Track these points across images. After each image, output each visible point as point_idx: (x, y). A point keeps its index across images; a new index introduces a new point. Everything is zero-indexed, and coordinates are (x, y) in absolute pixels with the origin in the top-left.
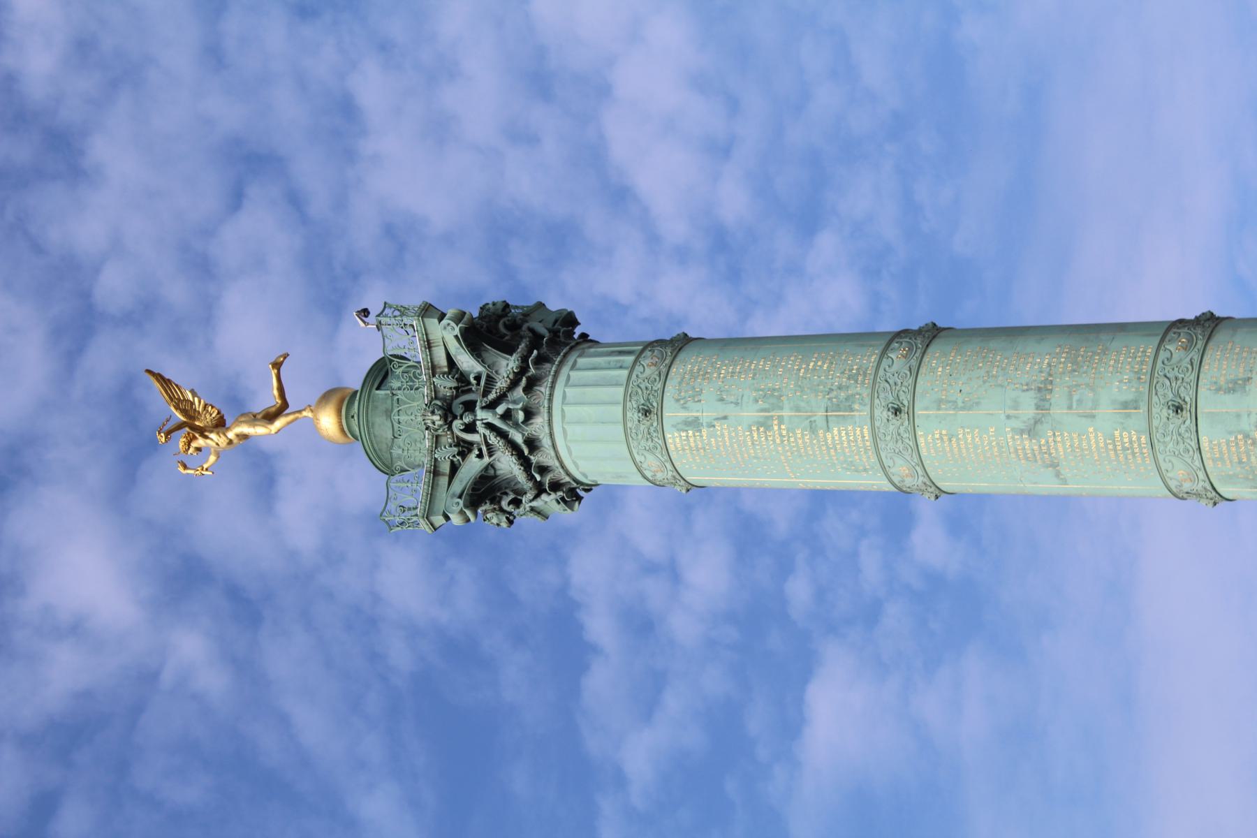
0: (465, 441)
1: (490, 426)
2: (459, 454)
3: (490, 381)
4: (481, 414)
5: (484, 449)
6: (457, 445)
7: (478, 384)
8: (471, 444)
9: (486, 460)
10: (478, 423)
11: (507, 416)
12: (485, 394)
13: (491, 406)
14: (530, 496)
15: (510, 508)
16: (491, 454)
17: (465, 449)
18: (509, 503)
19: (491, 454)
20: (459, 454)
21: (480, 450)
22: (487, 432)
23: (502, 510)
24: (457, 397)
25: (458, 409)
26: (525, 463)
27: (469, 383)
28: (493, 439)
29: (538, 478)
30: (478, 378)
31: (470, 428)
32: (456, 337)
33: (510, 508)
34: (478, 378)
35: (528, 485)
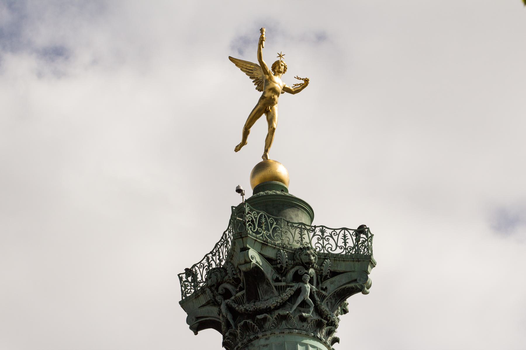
0: (287, 272)
1: (299, 292)
2: (282, 266)
3: (323, 297)
4: (308, 286)
5: (283, 284)
6: (286, 268)
7: (322, 289)
8: (285, 275)
9: (273, 284)
10: (301, 284)
11: (304, 304)
12: (318, 293)
13: (311, 296)
14: (235, 306)
16: (279, 289)
17: (281, 271)
18: (226, 289)
19: (279, 289)
20: (282, 266)
21: (280, 281)
22: (294, 289)
23: (219, 284)
24: (316, 272)
25: (311, 271)
26: (269, 311)
27: (322, 282)
28: (289, 292)
29: (259, 317)
30: (325, 289)
31: (298, 278)
32: (355, 281)
34: (325, 289)
35: (250, 307)
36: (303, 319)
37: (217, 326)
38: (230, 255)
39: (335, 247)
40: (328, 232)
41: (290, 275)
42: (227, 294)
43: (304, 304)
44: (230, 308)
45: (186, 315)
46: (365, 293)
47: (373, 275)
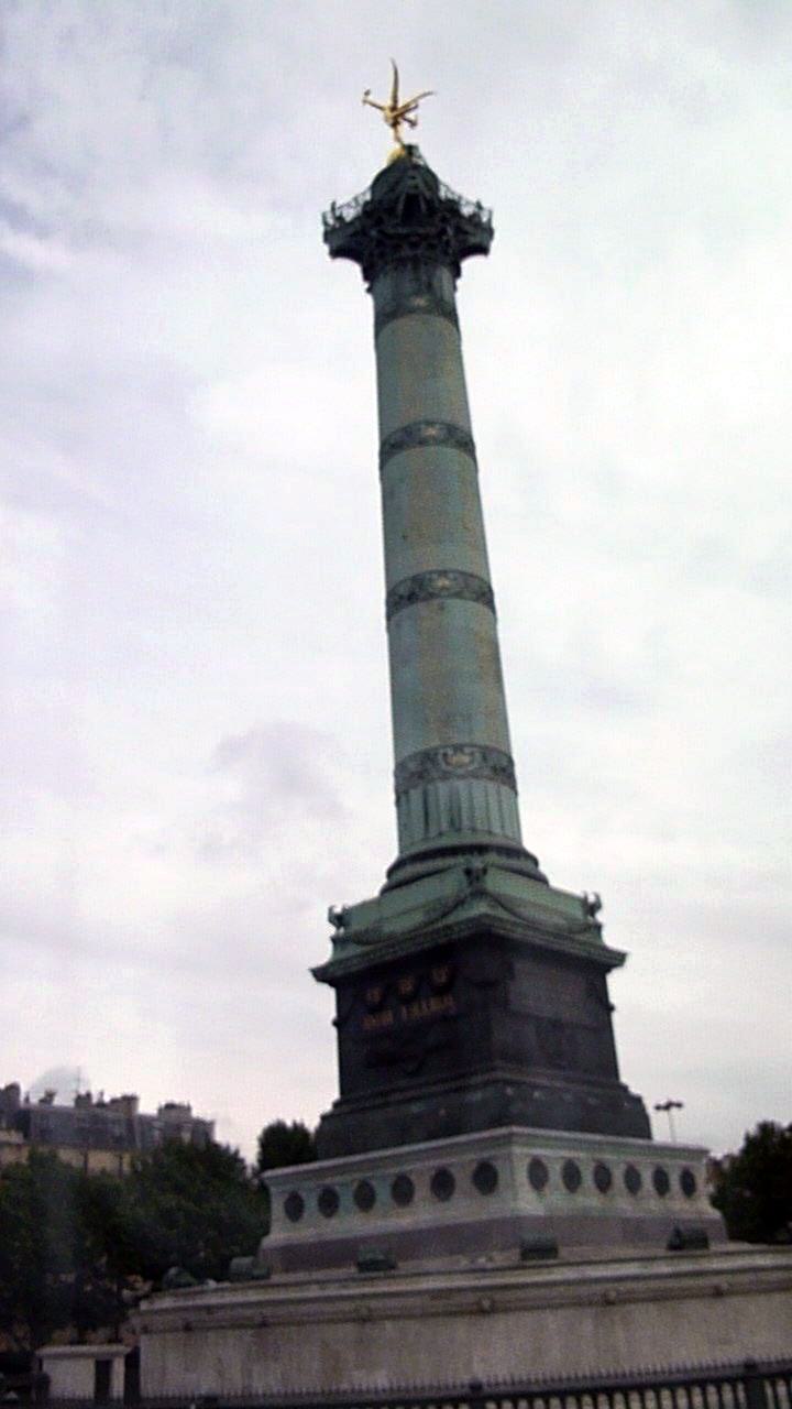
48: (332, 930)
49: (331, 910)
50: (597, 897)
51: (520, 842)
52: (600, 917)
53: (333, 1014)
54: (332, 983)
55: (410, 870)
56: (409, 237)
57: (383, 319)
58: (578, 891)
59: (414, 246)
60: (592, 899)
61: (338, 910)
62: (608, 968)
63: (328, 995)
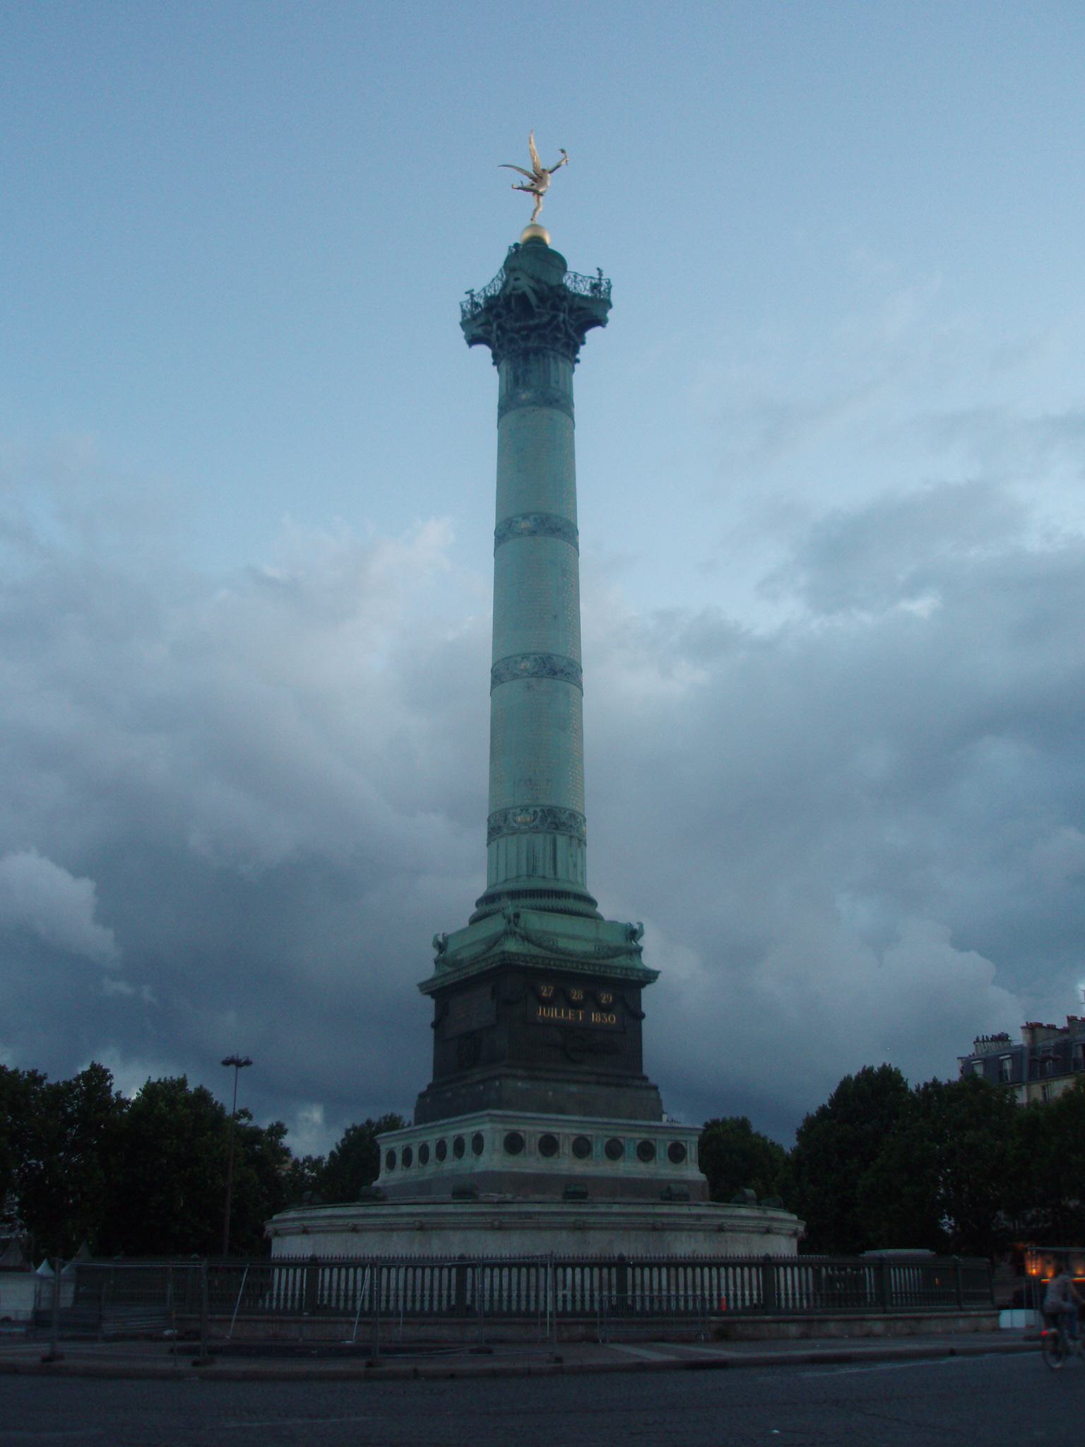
1: (555, 317)
11: (557, 328)
13: (564, 322)
15: (494, 312)
17: (542, 300)
33: (494, 312)
36: (556, 339)
37: (487, 342)
38: (505, 285)
39: (584, 289)
40: (579, 278)
41: (549, 304)
42: (498, 316)
43: (557, 328)
44: (500, 327)
45: (463, 333)
46: (603, 326)
47: (610, 314)
48: (435, 953)
49: (436, 936)
50: (641, 925)
51: (584, 885)
52: (640, 943)
53: (431, 1017)
54: (433, 994)
55: (487, 908)
56: (535, 321)
57: (506, 406)
58: (623, 920)
59: (526, 338)
60: (636, 927)
61: (440, 939)
62: (643, 984)
63: (430, 1002)
